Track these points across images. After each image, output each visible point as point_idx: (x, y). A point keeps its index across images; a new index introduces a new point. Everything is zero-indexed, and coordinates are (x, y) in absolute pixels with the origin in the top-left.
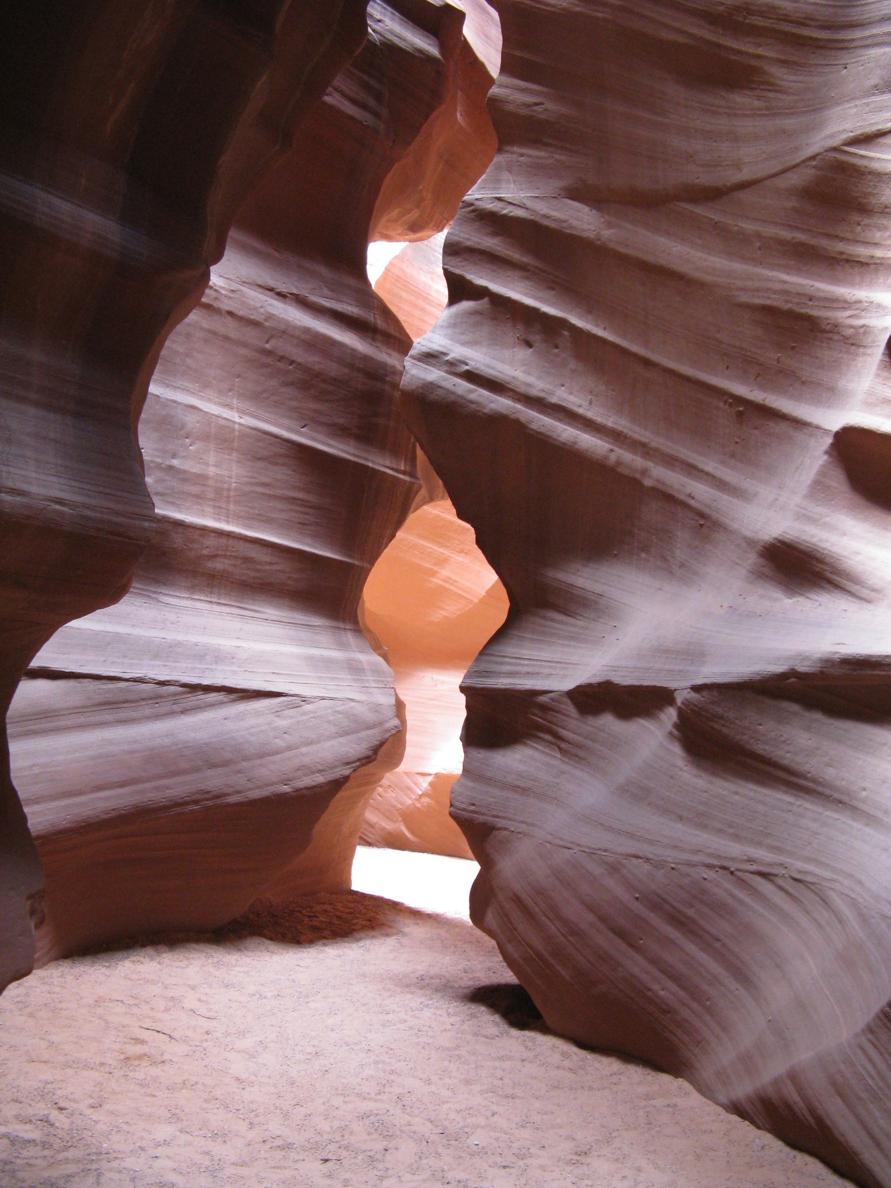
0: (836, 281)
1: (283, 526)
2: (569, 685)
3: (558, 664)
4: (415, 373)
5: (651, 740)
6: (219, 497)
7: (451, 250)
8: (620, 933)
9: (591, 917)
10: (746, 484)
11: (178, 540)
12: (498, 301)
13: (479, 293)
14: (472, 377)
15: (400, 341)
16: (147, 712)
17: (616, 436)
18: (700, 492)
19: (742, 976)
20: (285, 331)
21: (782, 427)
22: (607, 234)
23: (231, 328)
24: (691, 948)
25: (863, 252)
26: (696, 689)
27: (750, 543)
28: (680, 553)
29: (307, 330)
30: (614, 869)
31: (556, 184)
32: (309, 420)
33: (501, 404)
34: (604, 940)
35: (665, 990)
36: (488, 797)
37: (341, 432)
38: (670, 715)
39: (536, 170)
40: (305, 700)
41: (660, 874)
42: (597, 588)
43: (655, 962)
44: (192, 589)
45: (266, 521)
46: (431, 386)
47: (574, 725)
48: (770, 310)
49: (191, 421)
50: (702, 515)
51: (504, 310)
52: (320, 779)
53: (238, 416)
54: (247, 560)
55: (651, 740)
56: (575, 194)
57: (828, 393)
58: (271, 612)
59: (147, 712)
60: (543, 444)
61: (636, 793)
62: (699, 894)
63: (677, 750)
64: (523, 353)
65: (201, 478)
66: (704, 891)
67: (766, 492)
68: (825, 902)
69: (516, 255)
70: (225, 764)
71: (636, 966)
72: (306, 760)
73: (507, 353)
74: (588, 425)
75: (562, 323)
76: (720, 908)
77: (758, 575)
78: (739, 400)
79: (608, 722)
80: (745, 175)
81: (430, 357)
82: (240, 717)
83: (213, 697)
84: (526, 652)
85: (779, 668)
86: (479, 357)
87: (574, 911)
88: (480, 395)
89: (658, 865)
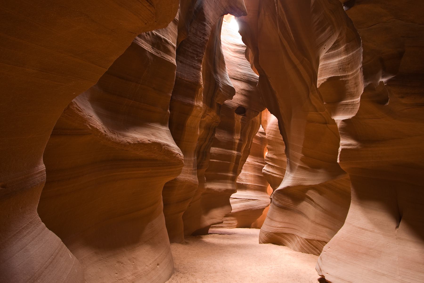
1: (258, 183)
4: (263, 171)
6: (251, 181)
11: (247, 186)
14: (267, 171)
17: (280, 175)
20: (256, 165)
23: (251, 165)
33: (269, 173)
39: (271, 153)
45: (256, 183)
49: (248, 175)
51: (269, 165)
53: (253, 174)
60: (273, 176)
65: (249, 180)
74: (277, 174)
81: (264, 170)
86: (268, 170)
88: (268, 173)
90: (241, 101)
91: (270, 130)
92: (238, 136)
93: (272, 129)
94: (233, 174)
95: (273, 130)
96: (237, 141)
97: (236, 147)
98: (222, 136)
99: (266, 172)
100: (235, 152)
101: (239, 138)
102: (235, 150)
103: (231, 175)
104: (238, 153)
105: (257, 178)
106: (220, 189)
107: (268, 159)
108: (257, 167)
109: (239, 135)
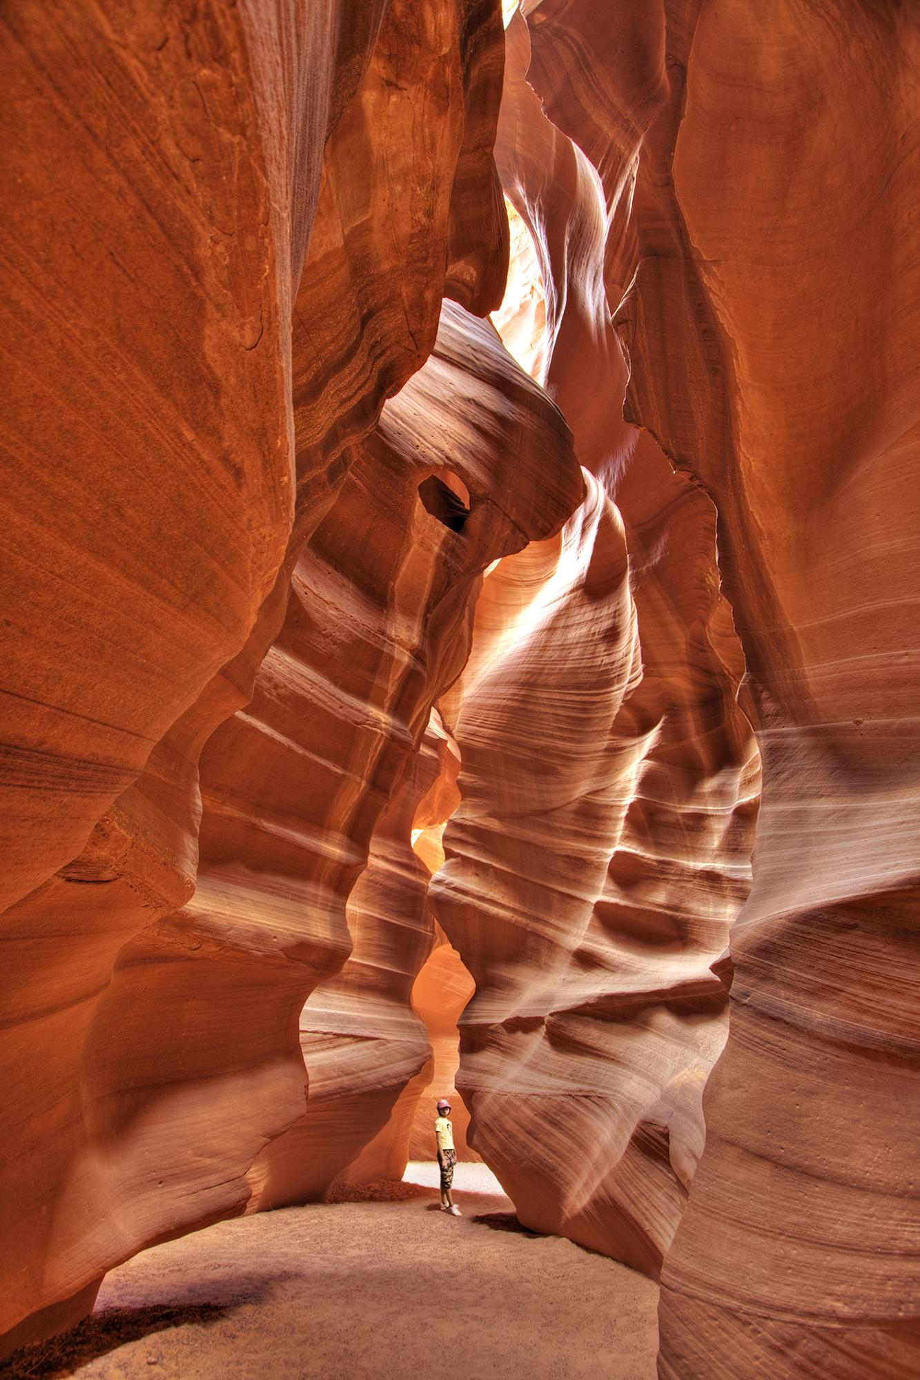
0: (590, 844)
2: (502, 1020)
3: (497, 1013)
4: (433, 889)
5: (537, 1042)
7: (446, 838)
8: (530, 1133)
9: (517, 1127)
10: (566, 927)
12: (465, 858)
13: (457, 855)
14: (456, 889)
15: (428, 875)
16: (318, 1047)
17: (514, 910)
18: (550, 932)
19: (582, 1146)
21: (577, 903)
22: (504, 830)
24: (561, 1136)
25: (599, 833)
26: (551, 1015)
27: (569, 951)
28: (544, 959)
29: (387, 871)
30: (526, 1101)
31: (484, 812)
32: (386, 909)
33: (467, 899)
34: (523, 1137)
35: (552, 1160)
36: (472, 1076)
37: (401, 914)
38: (543, 1029)
39: (475, 807)
40: (388, 1041)
41: (544, 1101)
42: (512, 976)
43: (545, 1145)
44: (338, 989)
46: (439, 894)
47: (505, 1038)
48: (568, 857)
50: (551, 942)
51: (466, 861)
52: (395, 1081)
54: (362, 974)
55: (537, 1042)
56: (491, 815)
57: (592, 889)
58: (372, 999)
59: (318, 1047)
60: (484, 915)
61: (532, 1066)
62: (561, 1109)
63: (547, 1043)
64: (475, 879)
66: (563, 1108)
67: (574, 930)
68: (611, 1105)
69: (470, 840)
70: (353, 1073)
71: (538, 1149)
72: (389, 1072)
73: (468, 879)
75: (490, 866)
76: (571, 1115)
77: (573, 965)
78: (561, 893)
79: (520, 1036)
80: (554, 805)
81: (439, 882)
82: (359, 1050)
83: (347, 1040)
84: (482, 1007)
85: (581, 1003)
86: (458, 881)
87: (510, 1125)
88: (459, 896)
89: (544, 1097)
90: (461, 448)
91: (481, 707)
92: (410, 628)
93: (491, 702)
94: (349, 849)
95: (494, 708)
96: (405, 658)
97: (391, 688)
98: (328, 598)
99: (452, 893)
100: (383, 717)
101: (416, 640)
102: (379, 704)
103: (334, 849)
104: (398, 724)
105: (375, 934)
106: (261, 937)
107: (459, 835)
108: (380, 879)
109: (417, 627)
